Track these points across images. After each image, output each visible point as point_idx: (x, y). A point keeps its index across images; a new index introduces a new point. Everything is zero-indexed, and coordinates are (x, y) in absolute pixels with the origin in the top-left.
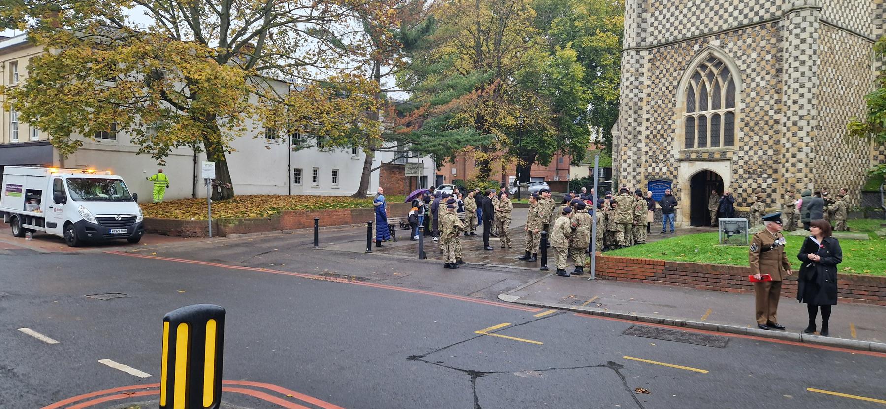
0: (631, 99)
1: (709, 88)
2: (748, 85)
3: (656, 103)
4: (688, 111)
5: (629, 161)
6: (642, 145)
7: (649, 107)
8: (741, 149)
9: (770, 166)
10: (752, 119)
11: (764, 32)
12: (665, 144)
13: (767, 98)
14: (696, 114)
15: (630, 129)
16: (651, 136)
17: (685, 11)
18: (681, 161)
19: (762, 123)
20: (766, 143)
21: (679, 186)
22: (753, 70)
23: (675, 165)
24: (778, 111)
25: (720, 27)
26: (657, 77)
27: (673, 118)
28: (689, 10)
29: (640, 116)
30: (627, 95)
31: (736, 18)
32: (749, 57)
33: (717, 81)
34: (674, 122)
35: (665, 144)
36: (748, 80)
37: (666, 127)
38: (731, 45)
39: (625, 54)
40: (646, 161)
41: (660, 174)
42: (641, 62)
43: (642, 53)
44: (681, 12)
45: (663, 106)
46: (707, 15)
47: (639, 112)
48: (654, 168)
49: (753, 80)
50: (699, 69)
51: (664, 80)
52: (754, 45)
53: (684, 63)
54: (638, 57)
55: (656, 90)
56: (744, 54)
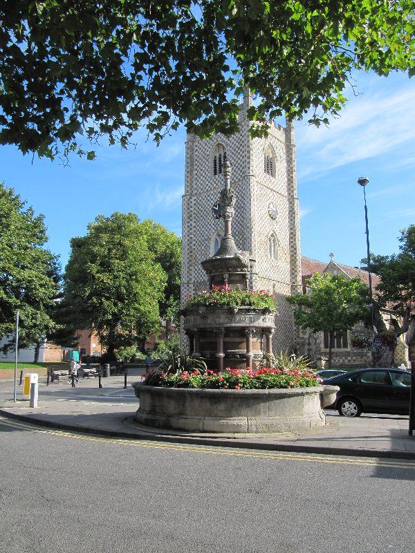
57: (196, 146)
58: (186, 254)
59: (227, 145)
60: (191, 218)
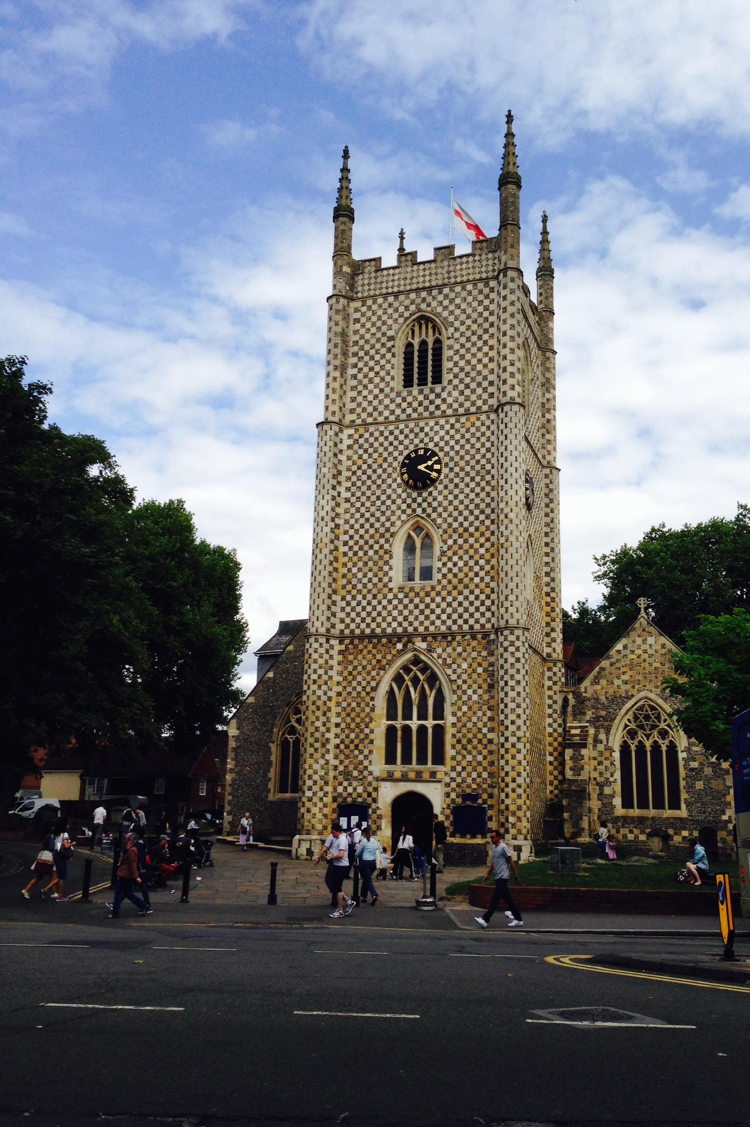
0: (319, 698)
1: (414, 695)
2: (460, 698)
3: (349, 705)
4: (388, 719)
5: (316, 777)
6: (330, 757)
7: (339, 709)
8: (453, 769)
9: (485, 791)
10: (464, 736)
11: (474, 643)
12: (361, 757)
13: (480, 714)
14: (399, 723)
15: (317, 735)
16: (342, 746)
17: (385, 602)
18: (383, 780)
19: (475, 741)
20: (480, 763)
21: (379, 812)
22: (465, 682)
23: (374, 784)
24: (491, 730)
25: (427, 628)
26: (350, 673)
27: (371, 726)
28: (390, 602)
29: (328, 719)
30: (314, 692)
31: (444, 622)
32: (459, 666)
33: (423, 689)
34: (372, 731)
36: (459, 692)
37: (362, 736)
38: (439, 650)
39: (312, 640)
40: (335, 778)
41: (355, 795)
42: (331, 652)
43: (332, 642)
44: (380, 603)
45: (358, 710)
46: (411, 612)
48: (345, 788)
49: (464, 692)
50: (401, 671)
51: (359, 678)
52: (464, 655)
53: (384, 662)
55: (349, 689)
56: (454, 663)
57: (357, 310)
58: (326, 562)
59: (448, 324)
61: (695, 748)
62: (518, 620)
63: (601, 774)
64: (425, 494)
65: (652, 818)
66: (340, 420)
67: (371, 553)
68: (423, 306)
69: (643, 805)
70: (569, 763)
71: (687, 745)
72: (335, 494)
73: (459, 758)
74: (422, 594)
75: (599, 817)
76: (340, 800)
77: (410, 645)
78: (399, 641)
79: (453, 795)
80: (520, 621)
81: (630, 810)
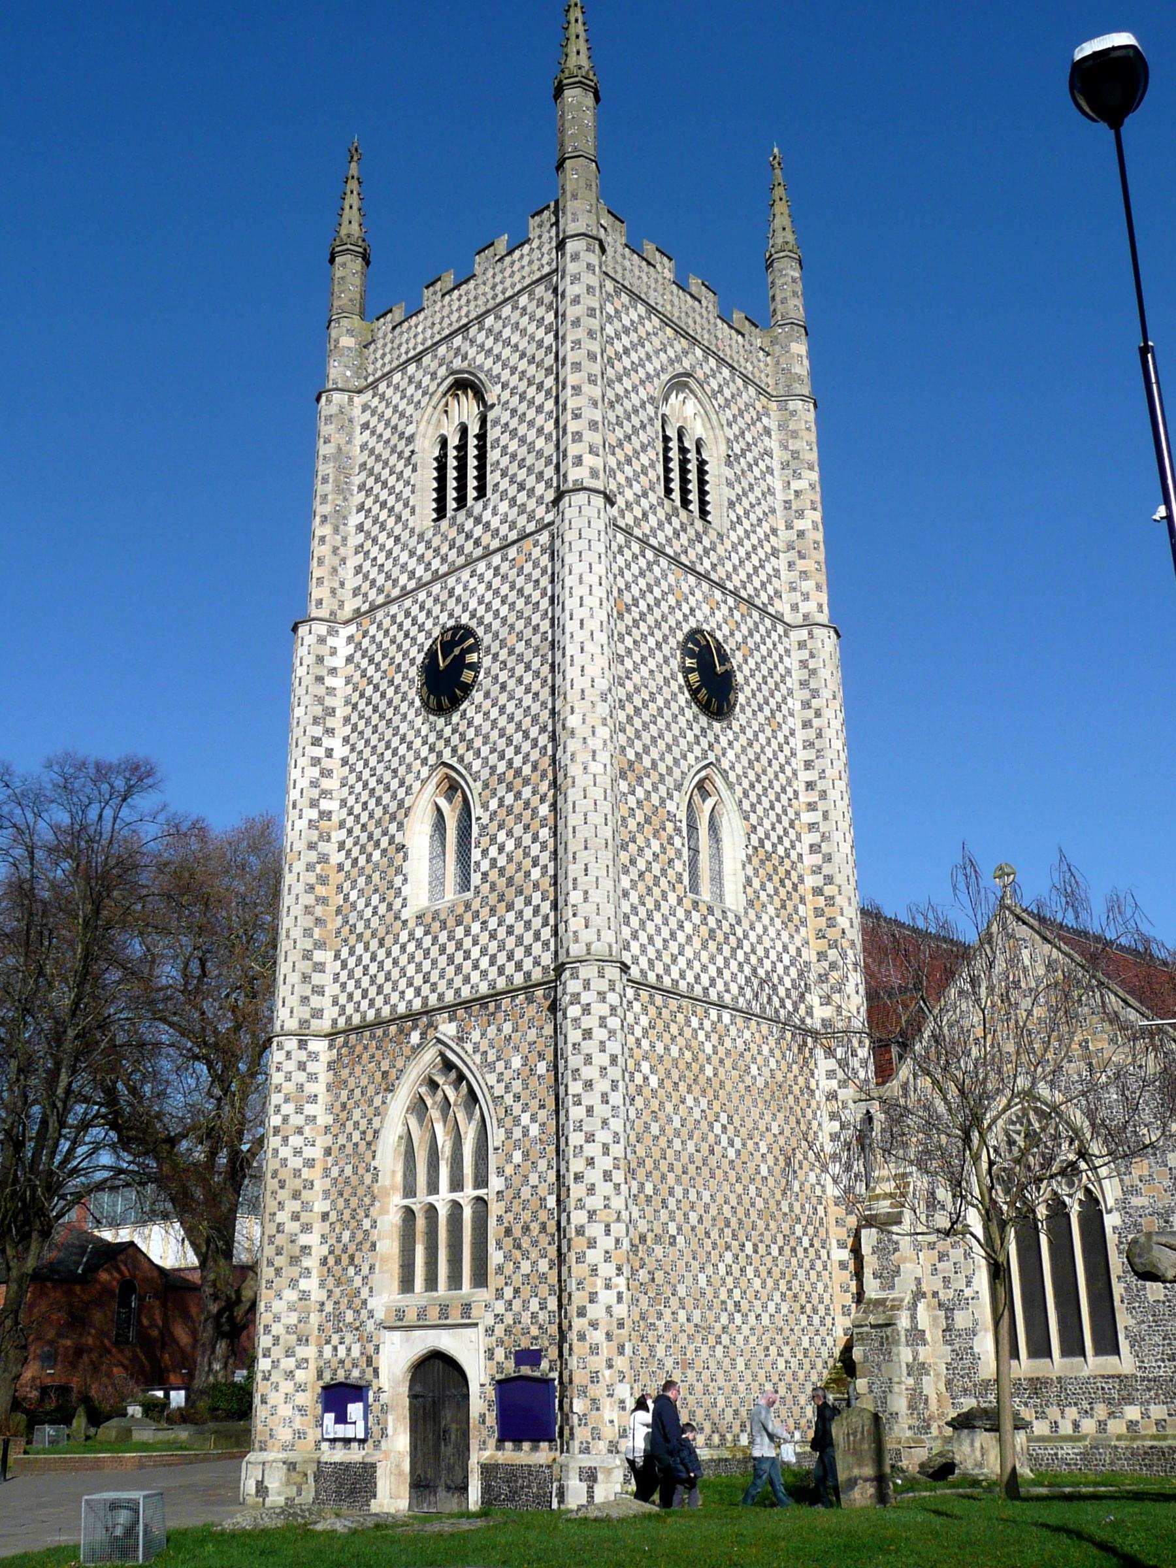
4: (406, 1196)
11: (531, 1011)
15: (280, 1240)
21: (384, 1398)
27: (373, 1212)
29: (307, 1207)
34: (374, 1225)
35: (358, 1282)
37: (360, 1236)
38: (476, 1036)
42: (311, 1067)
45: (354, 1180)
47: (306, 1195)
48: (335, 1349)
54: (302, 1056)
55: (342, 1140)
60: (331, 722)
61: (1136, 1201)
62: (588, 945)
63: (946, 1281)
64: (455, 718)
65: (1059, 1379)
66: (332, 613)
67: (376, 856)
68: (457, 364)
69: (1072, 1347)
70: (871, 1263)
71: (1120, 1195)
72: (319, 752)
73: (509, 1268)
74: (451, 922)
75: (949, 1383)
76: (327, 1377)
77: (431, 1032)
78: (415, 1028)
79: (500, 1354)
80: (593, 947)
81: (1044, 1362)
